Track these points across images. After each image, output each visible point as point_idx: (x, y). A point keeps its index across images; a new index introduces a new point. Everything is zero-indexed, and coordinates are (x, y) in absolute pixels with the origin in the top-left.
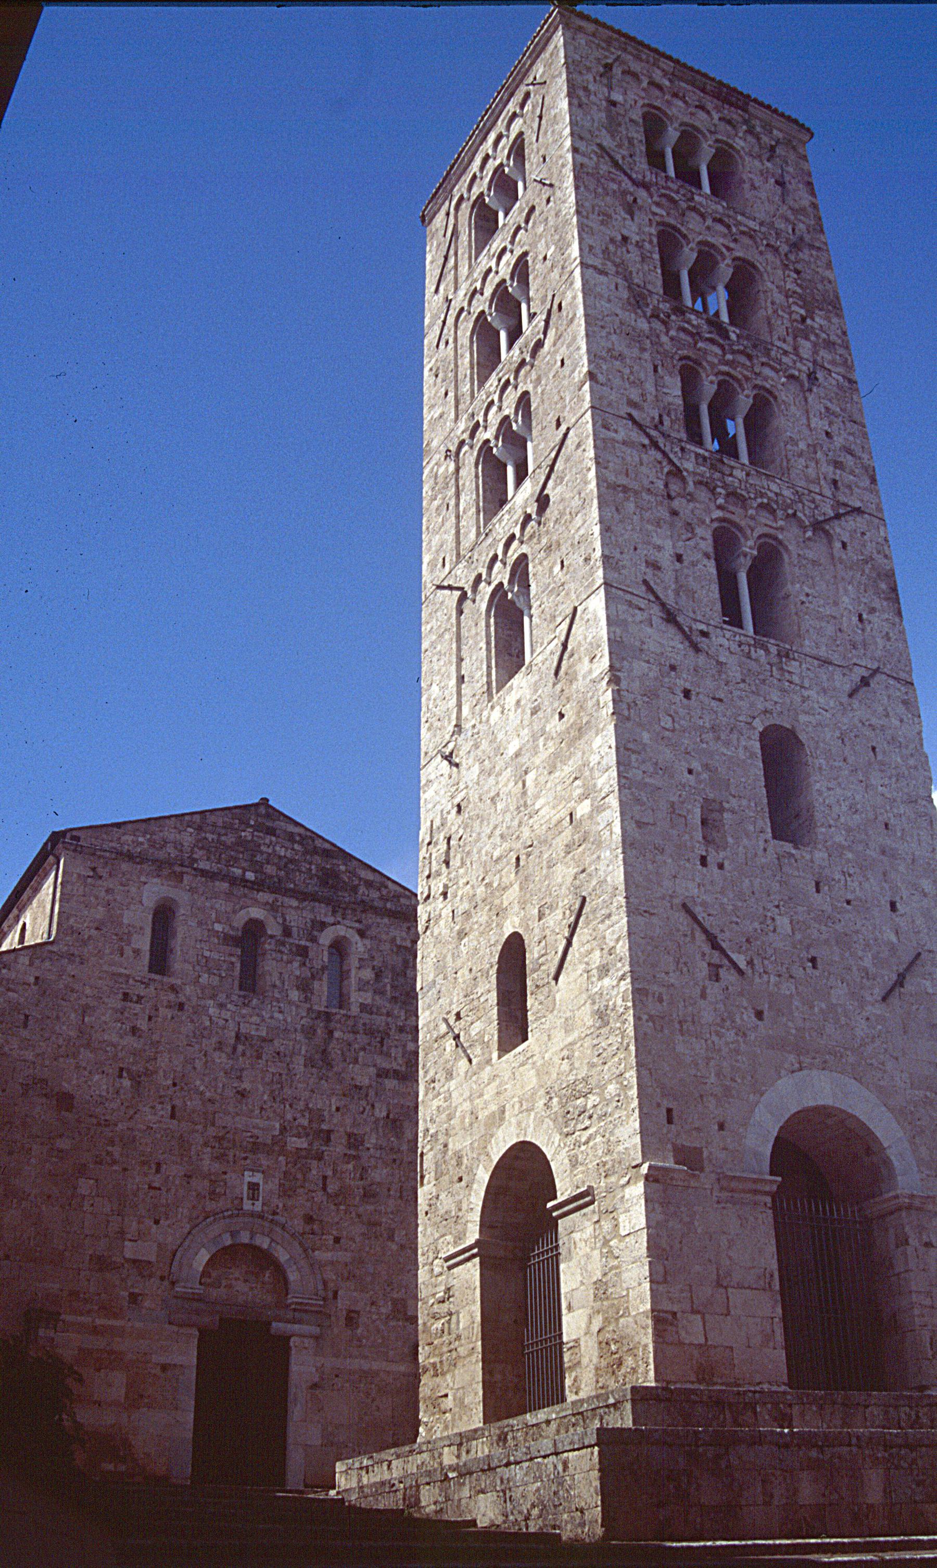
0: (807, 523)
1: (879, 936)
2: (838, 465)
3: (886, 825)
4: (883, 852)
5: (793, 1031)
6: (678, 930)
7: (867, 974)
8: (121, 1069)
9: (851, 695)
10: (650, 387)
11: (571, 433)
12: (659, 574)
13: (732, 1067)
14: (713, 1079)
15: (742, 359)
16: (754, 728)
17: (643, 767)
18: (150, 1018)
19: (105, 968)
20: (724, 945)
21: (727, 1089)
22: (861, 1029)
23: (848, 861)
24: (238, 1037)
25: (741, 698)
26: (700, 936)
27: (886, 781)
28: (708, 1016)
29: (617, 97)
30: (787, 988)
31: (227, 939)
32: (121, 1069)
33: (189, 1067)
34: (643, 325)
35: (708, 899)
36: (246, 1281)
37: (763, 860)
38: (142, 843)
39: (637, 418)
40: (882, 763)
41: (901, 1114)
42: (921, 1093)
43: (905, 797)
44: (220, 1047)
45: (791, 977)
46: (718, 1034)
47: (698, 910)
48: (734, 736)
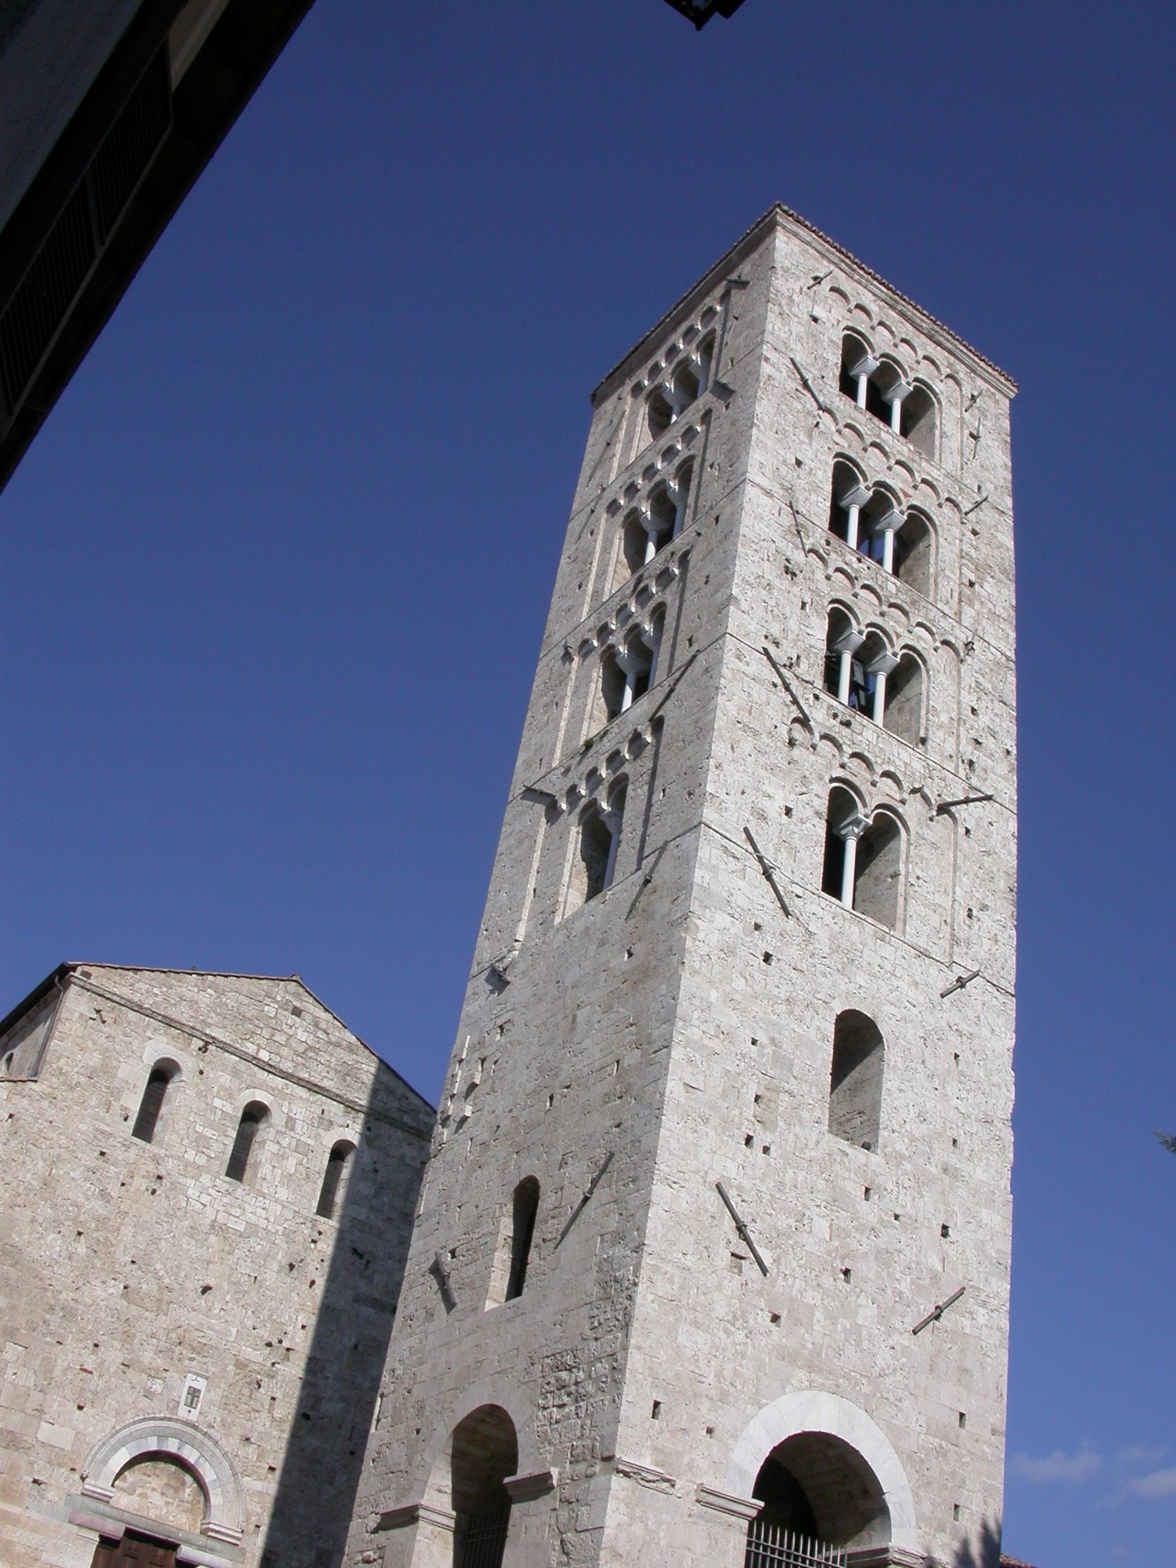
0: (933, 802)
3: (955, 1141)
4: (945, 1170)
5: (809, 1346)
6: (706, 1211)
9: (943, 996)
11: (701, 657)
13: (735, 1372)
14: (711, 1379)
16: (832, 1009)
17: (703, 1028)
20: (752, 1237)
22: (884, 1358)
23: (905, 1173)
25: (824, 975)
26: (729, 1224)
27: (964, 1095)
28: (720, 1310)
30: (813, 1297)
34: (798, 557)
35: (746, 1184)
36: (163, 1494)
37: (813, 1154)
38: (156, 995)
40: (962, 1073)
41: (909, 1459)
43: (981, 1116)
46: (726, 1331)
47: (732, 1194)
48: (809, 1014)
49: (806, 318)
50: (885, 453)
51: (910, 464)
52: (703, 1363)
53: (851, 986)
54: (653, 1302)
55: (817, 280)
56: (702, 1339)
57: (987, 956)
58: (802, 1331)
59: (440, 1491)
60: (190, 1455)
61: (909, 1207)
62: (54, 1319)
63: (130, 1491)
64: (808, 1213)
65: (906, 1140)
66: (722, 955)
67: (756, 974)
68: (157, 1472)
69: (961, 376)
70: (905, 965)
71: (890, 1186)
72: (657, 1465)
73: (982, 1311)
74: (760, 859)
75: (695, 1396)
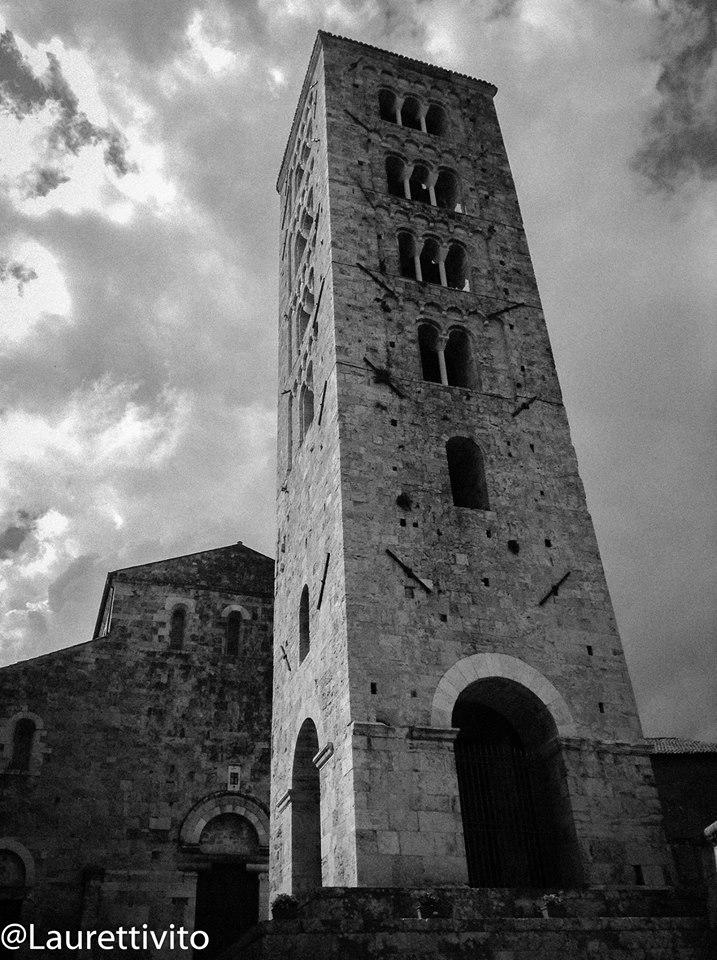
10: (374, 247)
15: (441, 225)
16: (442, 440)
20: (418, 575)
21: (418, 669)
22: (524, 623)
23: (512, 516)
29: (359, 81)
30: (465, 599)
34: (370, 211)
35: (406, 545)
44: (212, 690)
46: (411, 631)
47: (398, 554)
52: (399, 654)
55: (354, 65)
56: (397, 640)
60: (241, 811)
63: (212, 841)
71: (503, 526)
73: (586, 584)
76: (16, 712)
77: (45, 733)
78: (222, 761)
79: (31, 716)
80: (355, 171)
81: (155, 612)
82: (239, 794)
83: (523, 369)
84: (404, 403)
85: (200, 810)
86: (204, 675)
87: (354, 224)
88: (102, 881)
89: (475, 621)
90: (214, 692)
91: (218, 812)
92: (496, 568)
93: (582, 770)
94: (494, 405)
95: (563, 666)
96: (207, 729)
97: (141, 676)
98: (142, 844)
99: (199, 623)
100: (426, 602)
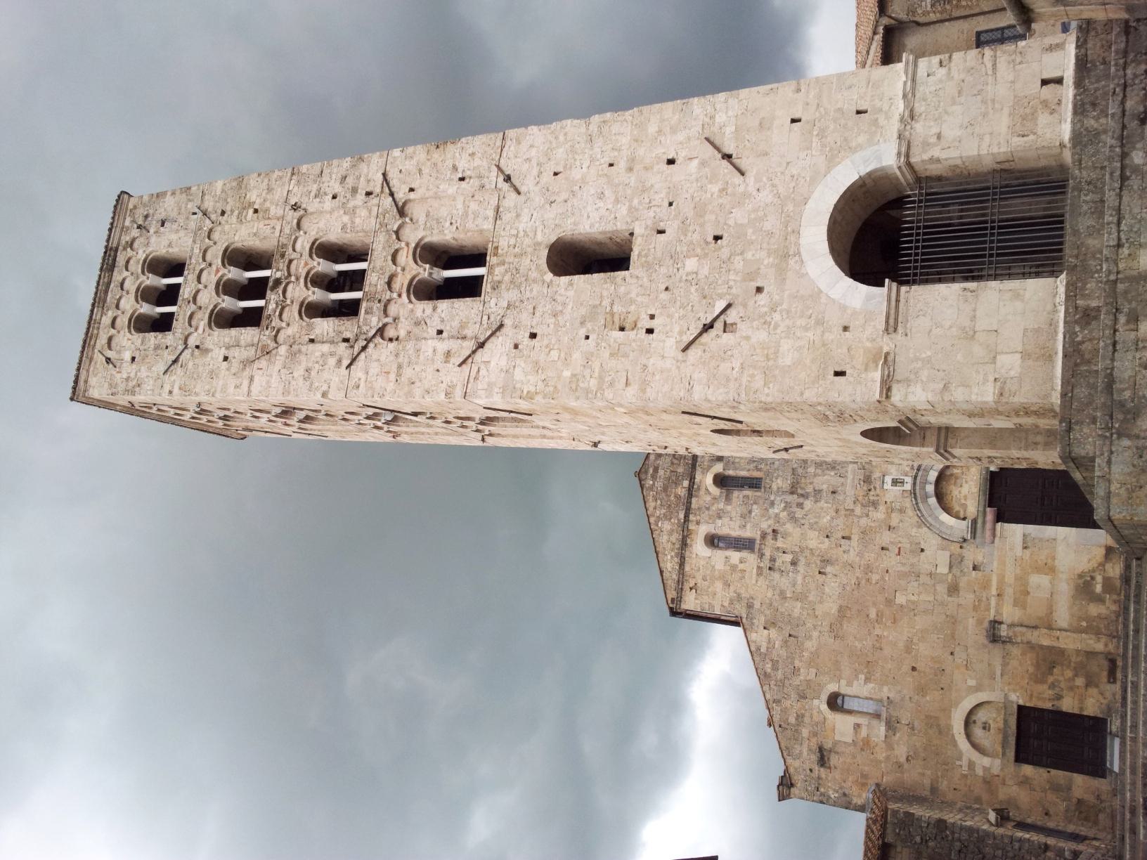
0: (400, 222)
1: (694, 176)
2: (354, 191)
3: (611, 165)
4: (630, 169)
5: (771, 260)
6: (701, 357)
7: (723, 190)
8: (820, 573)
9: (519, 193)
10: (326, 348)
12: (453, 351)
13: (801, 317)
14: (810, 334)
15: (293, 267)
16: (551, 281)
17: (588, 377)
18: (784, 552)
19: (754, 582)
22: (766, 196)
23: (640, 203)
24: (792, 493)
25: (531, 290)
26: (706, 338)
27: (578, 163)
29: (127, 356)
30: (738, 263)
31: (728, 499)
32: (820, 573)
33: (815, 526)
34: (283, 350)
35: (677, 329)
37: (645, 280)
38: (672, 557)
39: (349, 362)
40: (565, 167)
41: (832, 162)
42: (815, 140)
44: (800, 505)
45: (729, 259)
46: (776, 328)
48: (559, 298)
49: (134, 366)
50: (198, 291)
51: (197, 272)
53: (533, 268)
54: (769, 388)
55: (108, 360)
56: (786, 345)
57: (485, 160)
58: (762, 267)
59: (924, 438)
61: (662, 195)
62: (875, 577)
63: (964, 506)
64: (684, 278)
65: (619, 206)
66: (540, 371)
67: (546, 342)
68: (949, 492)
69: (128, 238)
70: (508, 228)
71: (652, 214)
72: (877, 366)
73: (718, 119)
74: (474, 352)
75: (824, 345)
76: (820, 712)
77: (843, 682)
78: (878, 495)
79: (824, 697)
80: (235, 365)
81: (714, 567)
82: (915, 478)
83: (462, 179)
84: (507, 322)
85: (929, 519)
86: (784, 515)
87: (299, 372)
88: (1001, 623)
89: (763, 254)
90: (802, 504)
91: (933, 501)
92: (702, 225)
93: (933, 140)
94: (506, 217)
95: (814, 153)
96: (843, 512)
97: (783, 582)
98: (963, 583)
99: (726, 520)
100: (741, 309)
